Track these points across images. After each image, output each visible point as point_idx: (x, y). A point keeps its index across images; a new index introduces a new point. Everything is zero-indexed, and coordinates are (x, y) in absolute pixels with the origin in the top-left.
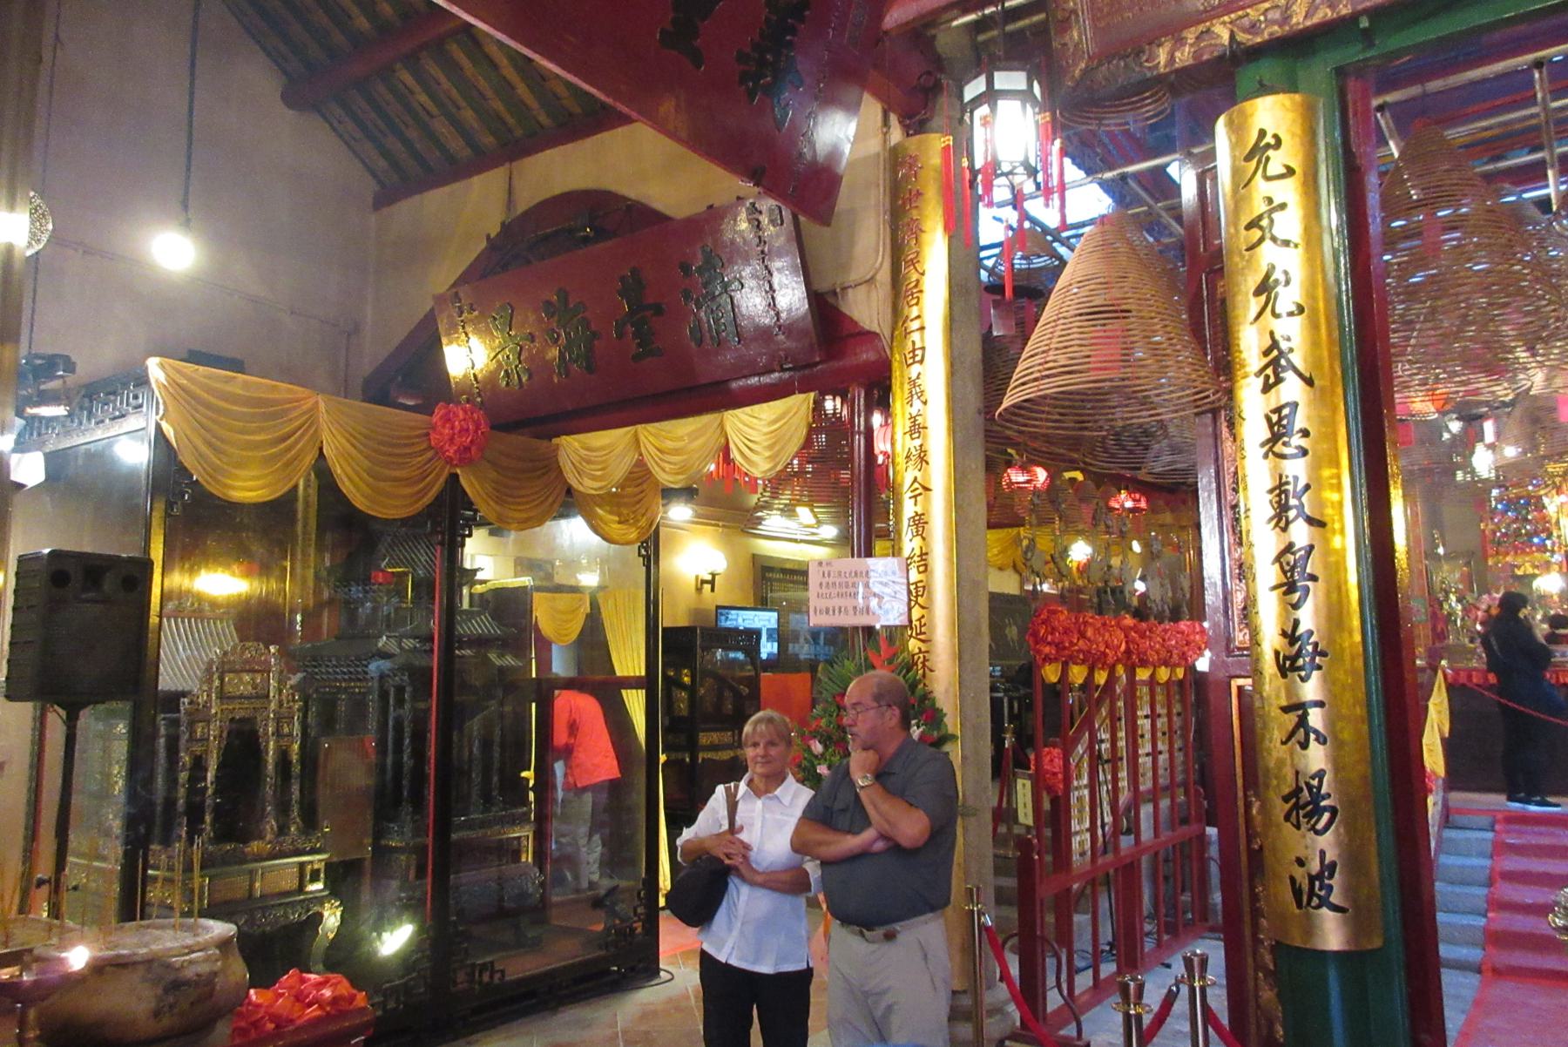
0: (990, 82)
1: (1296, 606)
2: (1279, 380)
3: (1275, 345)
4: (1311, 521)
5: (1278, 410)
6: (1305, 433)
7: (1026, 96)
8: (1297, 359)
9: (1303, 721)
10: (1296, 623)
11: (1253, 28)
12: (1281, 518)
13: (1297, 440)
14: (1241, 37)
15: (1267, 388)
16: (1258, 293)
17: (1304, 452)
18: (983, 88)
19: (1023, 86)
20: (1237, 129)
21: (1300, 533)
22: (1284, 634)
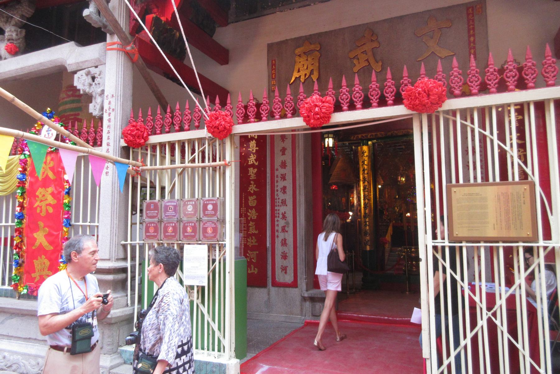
0: (328, 136)
1: (366, 209)
2: (365, 182)
3: (364, 178)
4: (368, 199)
5: (365, 186)
6: (368, 189)
7: (333, 138)
8: (367, 179)
9: (366, 224)
10: (366, 212)
11: (363, 137)
12: (364, 199)
13: (367, 190)
14: (362, 138)
15: (364, 183)
16: (363, 171)
17: (367, 191)
18: (327, 136)
19: (332, 136)
20: (362, 149)
21: (367, 201)
22: (364, 213)
